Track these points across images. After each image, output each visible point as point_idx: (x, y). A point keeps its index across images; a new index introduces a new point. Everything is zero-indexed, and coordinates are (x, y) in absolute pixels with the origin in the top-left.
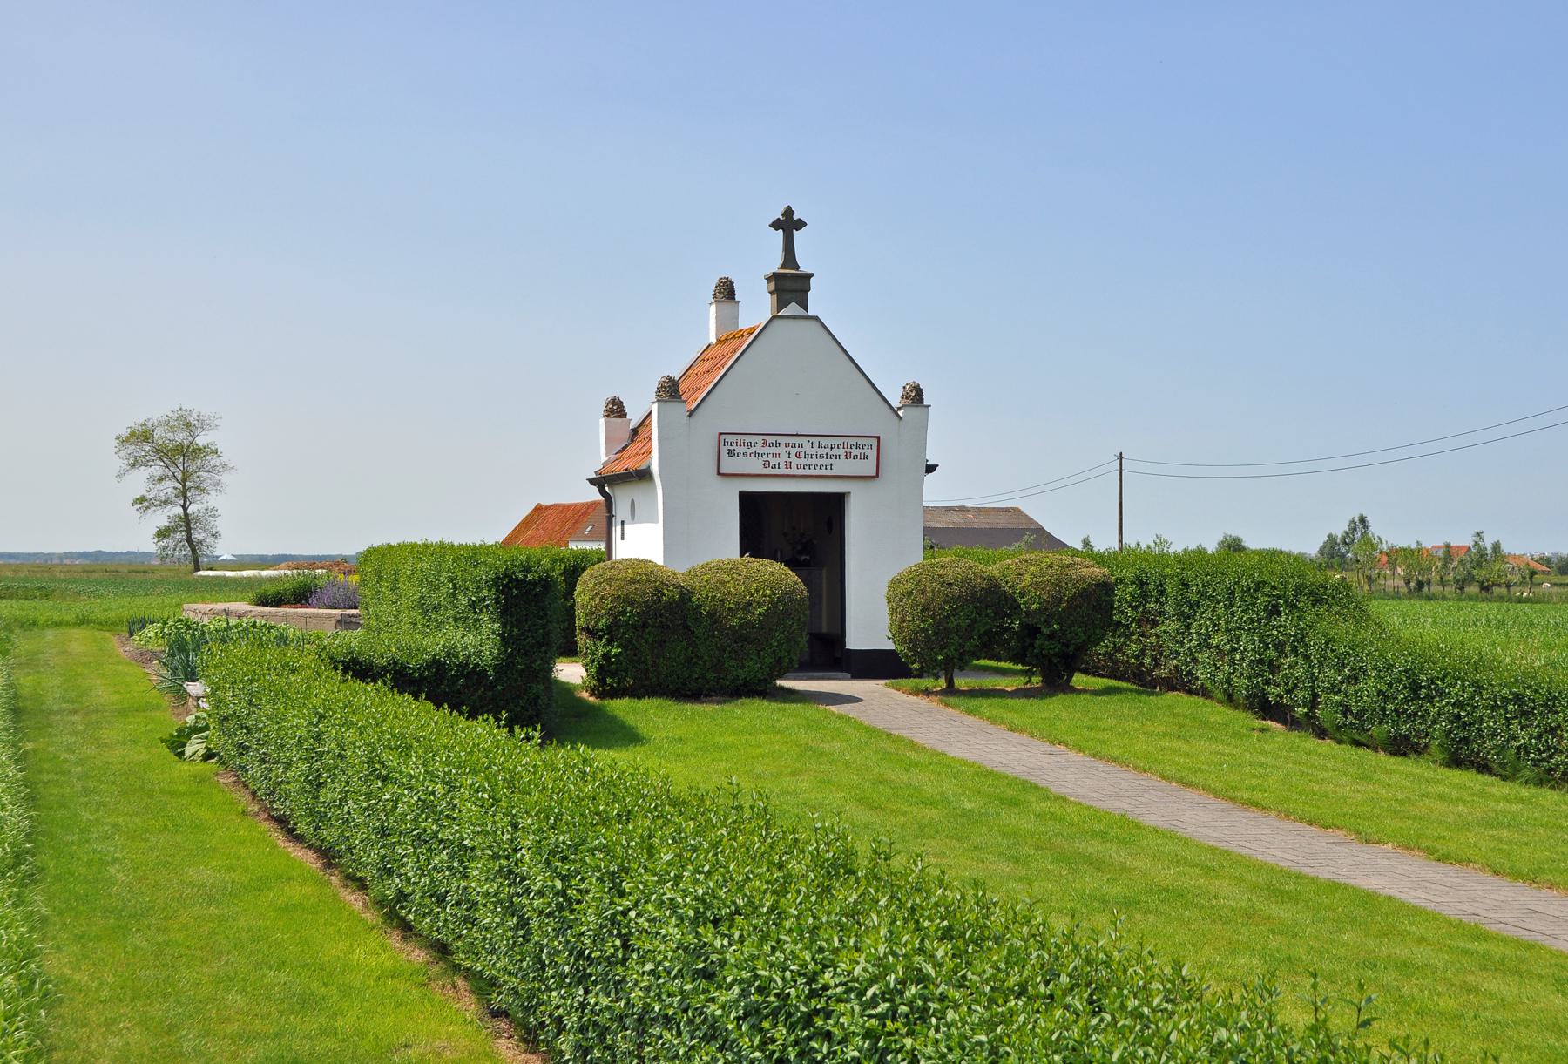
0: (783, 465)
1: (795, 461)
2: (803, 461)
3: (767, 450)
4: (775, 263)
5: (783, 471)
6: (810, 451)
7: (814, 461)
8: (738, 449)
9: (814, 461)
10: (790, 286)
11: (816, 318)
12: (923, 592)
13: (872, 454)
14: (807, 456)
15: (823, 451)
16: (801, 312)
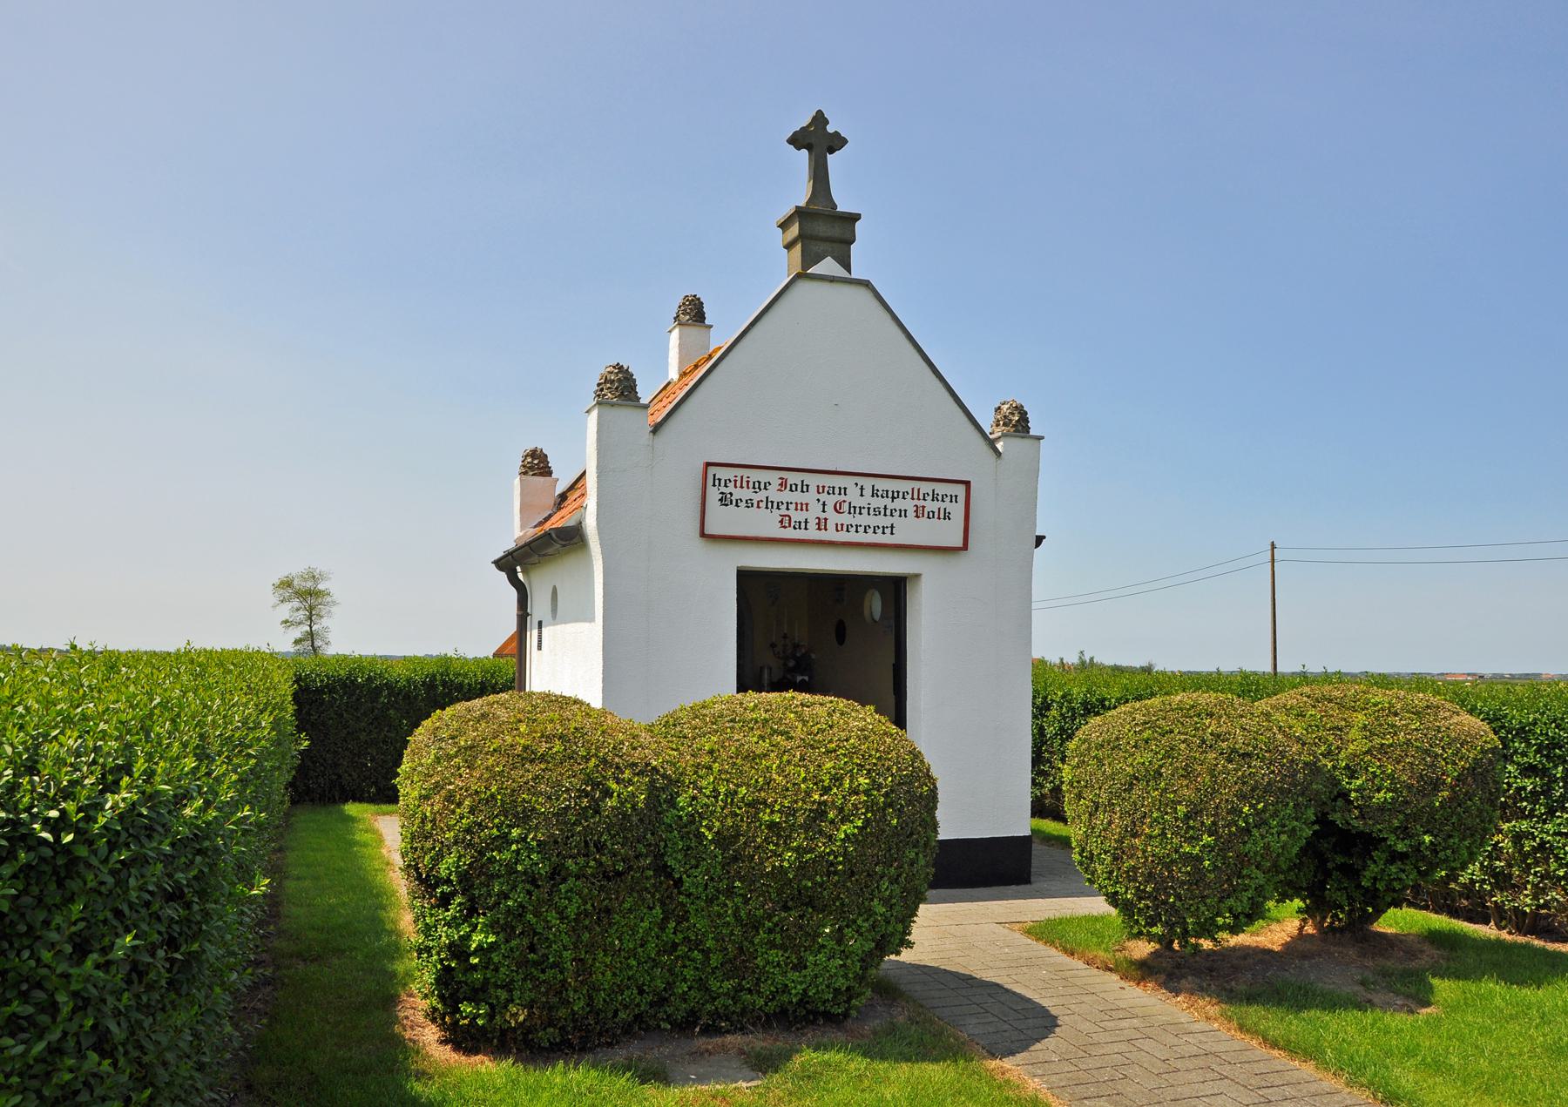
0: (812, 525)
1: (833, 518)
2: (846, 519)
3: (786, 496)
4: (801, 195)
5: (813, 533)
7: (864, 519)
8: (738, 493)
9: (864, 519)
10: (822, 231)
11: (866, 284)
12: (1188, 773)
13: (957, 510)
14: (853, 510)
15: (878, 503)
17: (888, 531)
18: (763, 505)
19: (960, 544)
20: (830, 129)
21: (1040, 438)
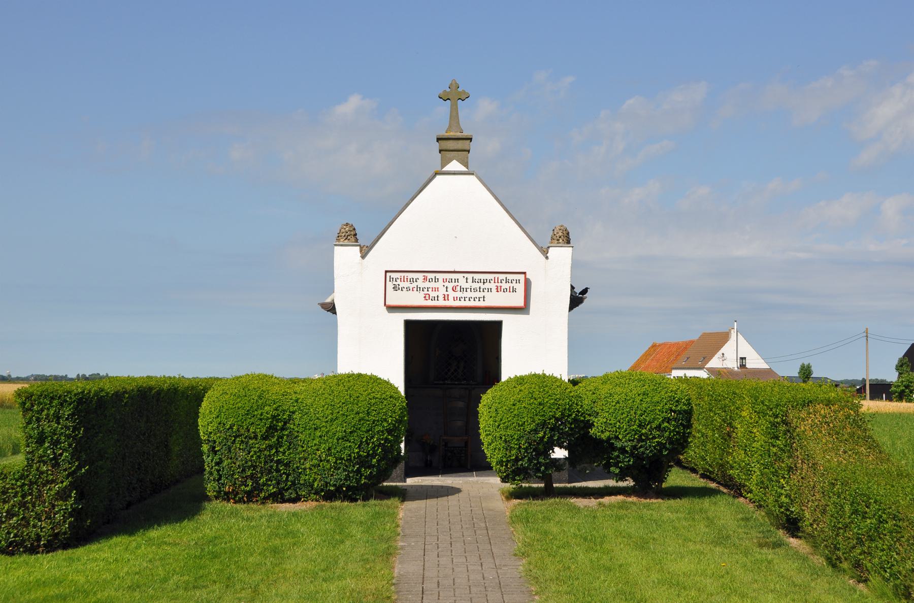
0: (441, 298)
2: (459, 294)
3: (427, 284)
5: (441, 303)
6: (465, 285)
7: (468, 294)
8: (402, 284)
13: (521, 288)
16: (464, 169)
19: (520, 303)
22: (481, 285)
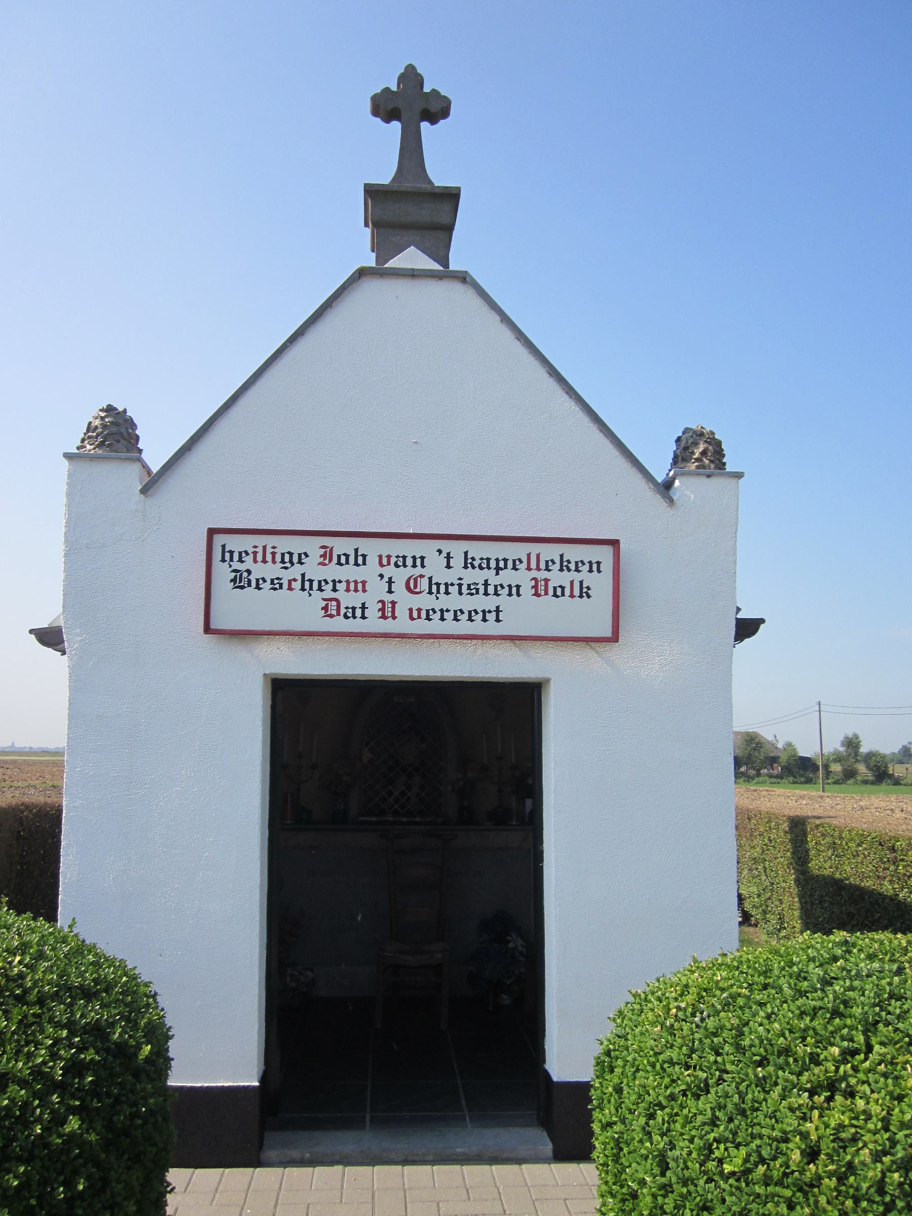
0: (373, 611)
1: (404, 601)
2: (425, 601)
3: (332, 572)
5: (374, 623)
6: (442, 576)
7: (453, 601)
9: (453, 601)
11: (463, 278)
13: (601, 584)
14: (434, 587)
16: (437, 267)
17: (491, 617)
18: (297, 585)
20: (427, 89)
21: (739, 475)
22: (490, 574)
